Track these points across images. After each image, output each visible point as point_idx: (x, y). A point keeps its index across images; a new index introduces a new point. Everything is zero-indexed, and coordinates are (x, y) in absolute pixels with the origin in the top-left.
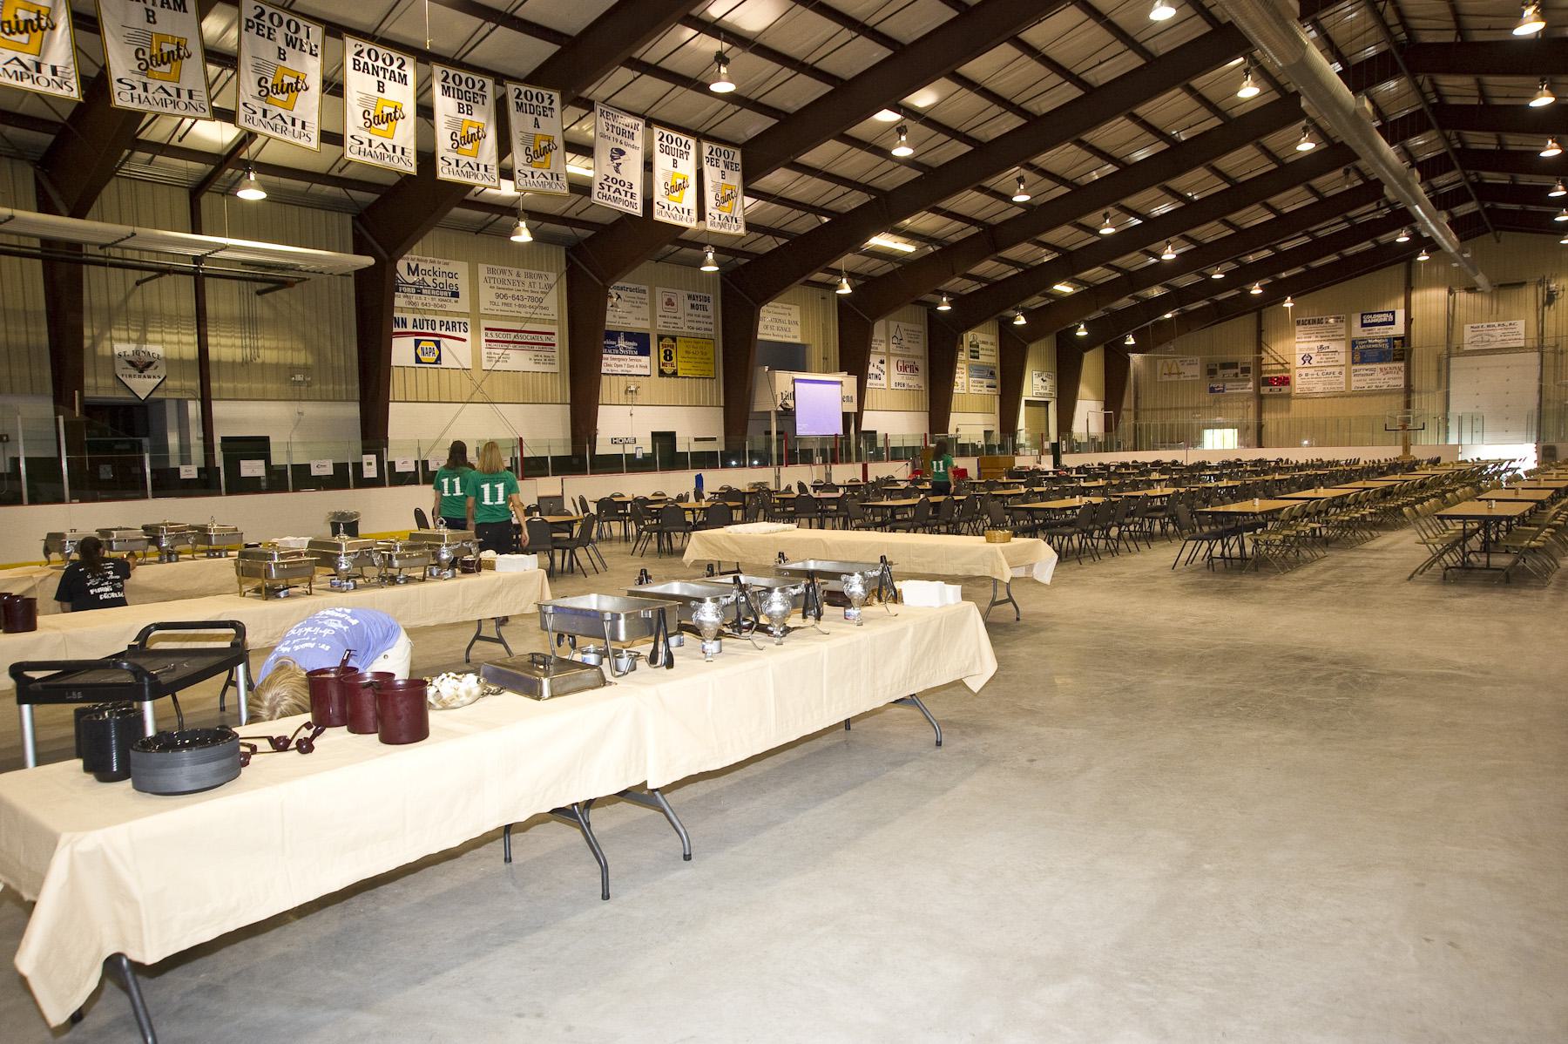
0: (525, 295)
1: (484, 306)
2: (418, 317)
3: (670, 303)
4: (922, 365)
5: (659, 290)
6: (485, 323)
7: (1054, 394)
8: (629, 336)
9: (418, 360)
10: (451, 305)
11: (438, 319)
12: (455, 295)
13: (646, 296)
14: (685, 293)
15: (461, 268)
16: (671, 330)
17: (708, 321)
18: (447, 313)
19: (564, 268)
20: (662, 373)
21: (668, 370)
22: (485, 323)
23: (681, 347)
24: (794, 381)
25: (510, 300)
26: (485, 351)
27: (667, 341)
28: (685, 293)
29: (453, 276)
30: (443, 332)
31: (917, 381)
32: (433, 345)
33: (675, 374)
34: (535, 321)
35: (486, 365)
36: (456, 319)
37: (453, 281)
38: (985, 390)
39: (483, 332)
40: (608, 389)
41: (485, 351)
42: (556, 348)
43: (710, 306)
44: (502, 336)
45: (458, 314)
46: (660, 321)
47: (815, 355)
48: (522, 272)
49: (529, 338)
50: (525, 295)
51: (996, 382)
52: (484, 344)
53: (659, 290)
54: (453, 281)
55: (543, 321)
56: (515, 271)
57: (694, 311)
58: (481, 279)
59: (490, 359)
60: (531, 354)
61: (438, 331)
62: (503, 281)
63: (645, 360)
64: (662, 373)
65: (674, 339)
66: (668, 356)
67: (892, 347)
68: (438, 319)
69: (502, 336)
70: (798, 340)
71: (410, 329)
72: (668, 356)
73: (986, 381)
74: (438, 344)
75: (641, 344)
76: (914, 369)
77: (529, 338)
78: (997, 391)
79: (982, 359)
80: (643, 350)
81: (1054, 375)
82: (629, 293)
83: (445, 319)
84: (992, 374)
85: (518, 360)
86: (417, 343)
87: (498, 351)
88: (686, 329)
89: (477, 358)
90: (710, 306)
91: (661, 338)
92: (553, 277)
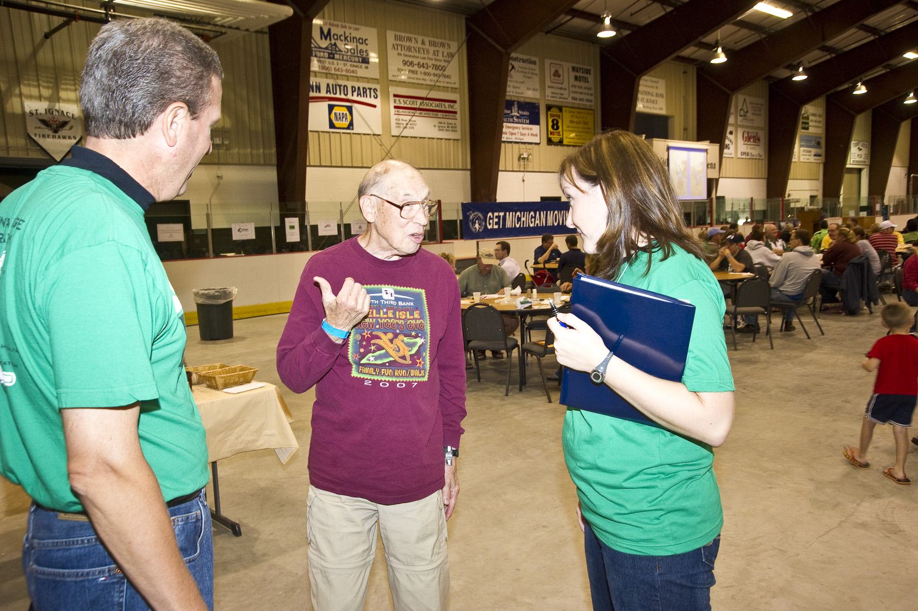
0: (430, 63)
3: (556, 74)
4: (763, 135)
5: (547, 62)
6: (393, 90)
7: (868, 162)
8: (523, 106)
9: (332, 125)
10: (362, 72)
11: (350, 84)
12: (366, 61)
13: (536, 67)
14: (570, 65)
15: (369, 33)
16: (557, 101)
17: (588, 93)
18: (358, 79)
19: (464, 37)
20: (550, 142)
21: (555, 138)
22: (393, 90)
23: (566, 119)
24: (668, 148)
25: (416, 68)
26: (393, 117)
27: (554, 111)
28: (570, 65)
29: (364, 41)
30: (355, 98)
31: (758, 151)
32: (345, 111)
33: (560, 143)
34: (439, 88)
35: (395, 132)
36: (367, 86)
38: (812, 159)
39: (392, 99)
40: (507, 156)
41: (393, 117)
42: (458, 116)
43: (591, 78)
44: (409, 103)
45: (368, 80)
46: (548, 92)
47: (677, 125)
48: (427, 40)
49: (434, 105)
50: (430, 63)
51: (822, 151)
53: (547, 62)
55: (445, 89)
56: (420, 39)
57: (577, 83)
58: (390, 46)
59: (398, 125)
60: (435, 121)
61: (350, 97)
62: (409, 49)
63: (535, 128)
64: (550, 142)
65: (560, 109)
66: (555, 126)
67: (740, 118)
68: (350, 84)
69: (409, 103)
70: (663, 112)
71: (323, 94)
72: (555, 126)
73: (814, 151)
74: (350, 109)
75: (531, 113)
76: (756, 139)
77: (434, 105)
78: (821, 160)
79: (811, 130)
80: (535, 120)
81: (868, 144)
82: (522, 64)
83: (356, 85)
84: (819, 144)
85: (424, 127)
86: (331, 108)
87: (405, 117)
88: (570, 100)
90: (591, 78)
91: (549, 108)
92: (454, 46)
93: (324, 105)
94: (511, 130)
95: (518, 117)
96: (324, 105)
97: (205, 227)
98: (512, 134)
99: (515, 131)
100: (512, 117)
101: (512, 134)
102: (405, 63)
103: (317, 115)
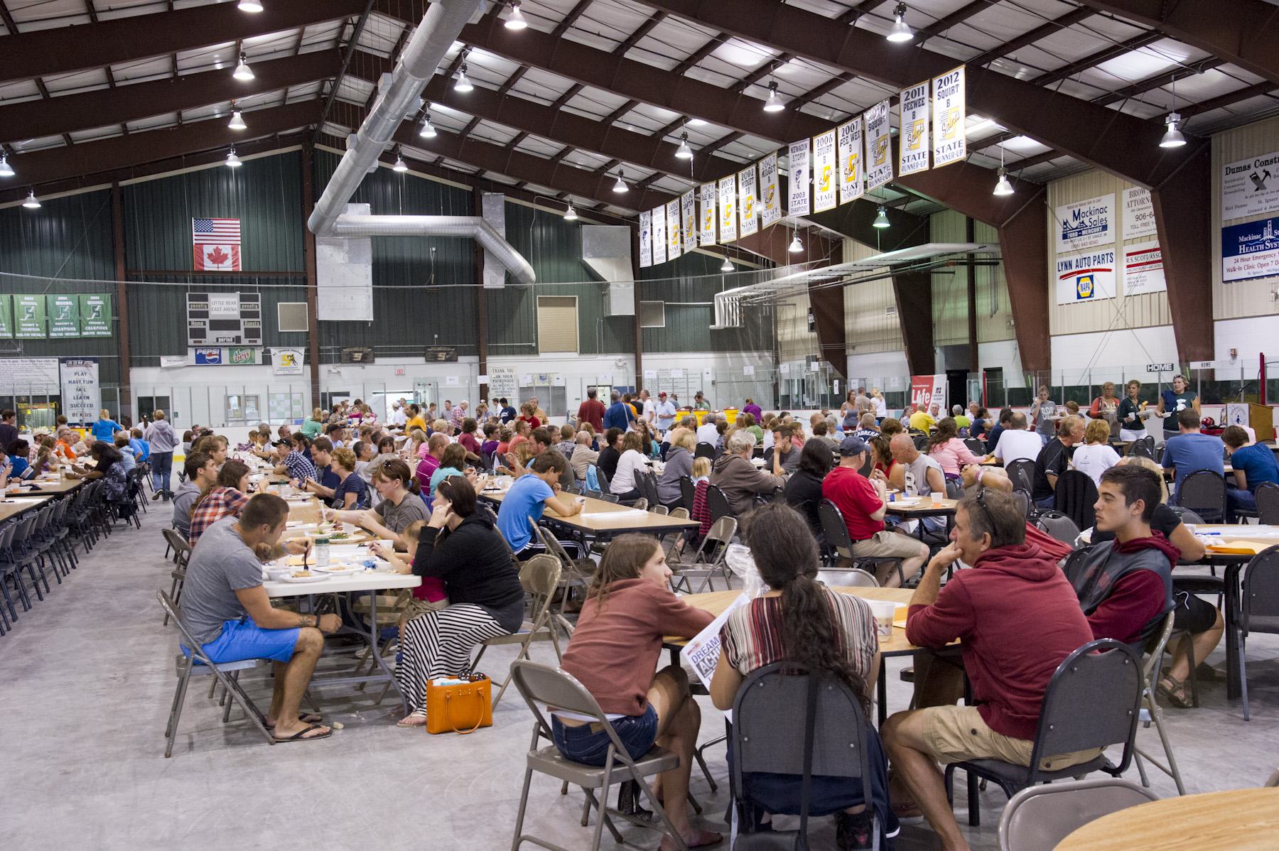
1: (1127, 232)
2: (1079, 257)
9: (1079, 297)
15: (1108, 201)
29: (1103, 210)
32: (1088, 281)
37: (1102, 216)
39: (1125, 258)
41: (1126, 277)
52: (1126, 270)
54: (1102, 216)
58: (1125, 205)
71: (1074, 269)
74: (1091, 278)
86: (1079, 280)
87: (1136, 274)
89: (1118, 286)
93: (1074, 279)
94: (1262, 261)
95: (1272, 241)
96: (1074, 279)
97: (1239, 378)
98: (1262, 266)
99: (1268, 260)
100: (1264, 242)
101: (1262, 266)
102: (1138, 218)
103: (1062, 291)
